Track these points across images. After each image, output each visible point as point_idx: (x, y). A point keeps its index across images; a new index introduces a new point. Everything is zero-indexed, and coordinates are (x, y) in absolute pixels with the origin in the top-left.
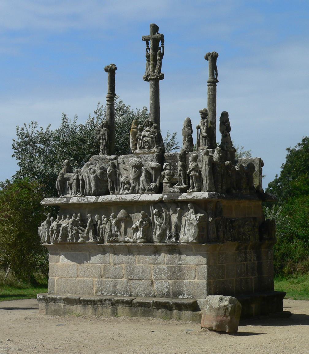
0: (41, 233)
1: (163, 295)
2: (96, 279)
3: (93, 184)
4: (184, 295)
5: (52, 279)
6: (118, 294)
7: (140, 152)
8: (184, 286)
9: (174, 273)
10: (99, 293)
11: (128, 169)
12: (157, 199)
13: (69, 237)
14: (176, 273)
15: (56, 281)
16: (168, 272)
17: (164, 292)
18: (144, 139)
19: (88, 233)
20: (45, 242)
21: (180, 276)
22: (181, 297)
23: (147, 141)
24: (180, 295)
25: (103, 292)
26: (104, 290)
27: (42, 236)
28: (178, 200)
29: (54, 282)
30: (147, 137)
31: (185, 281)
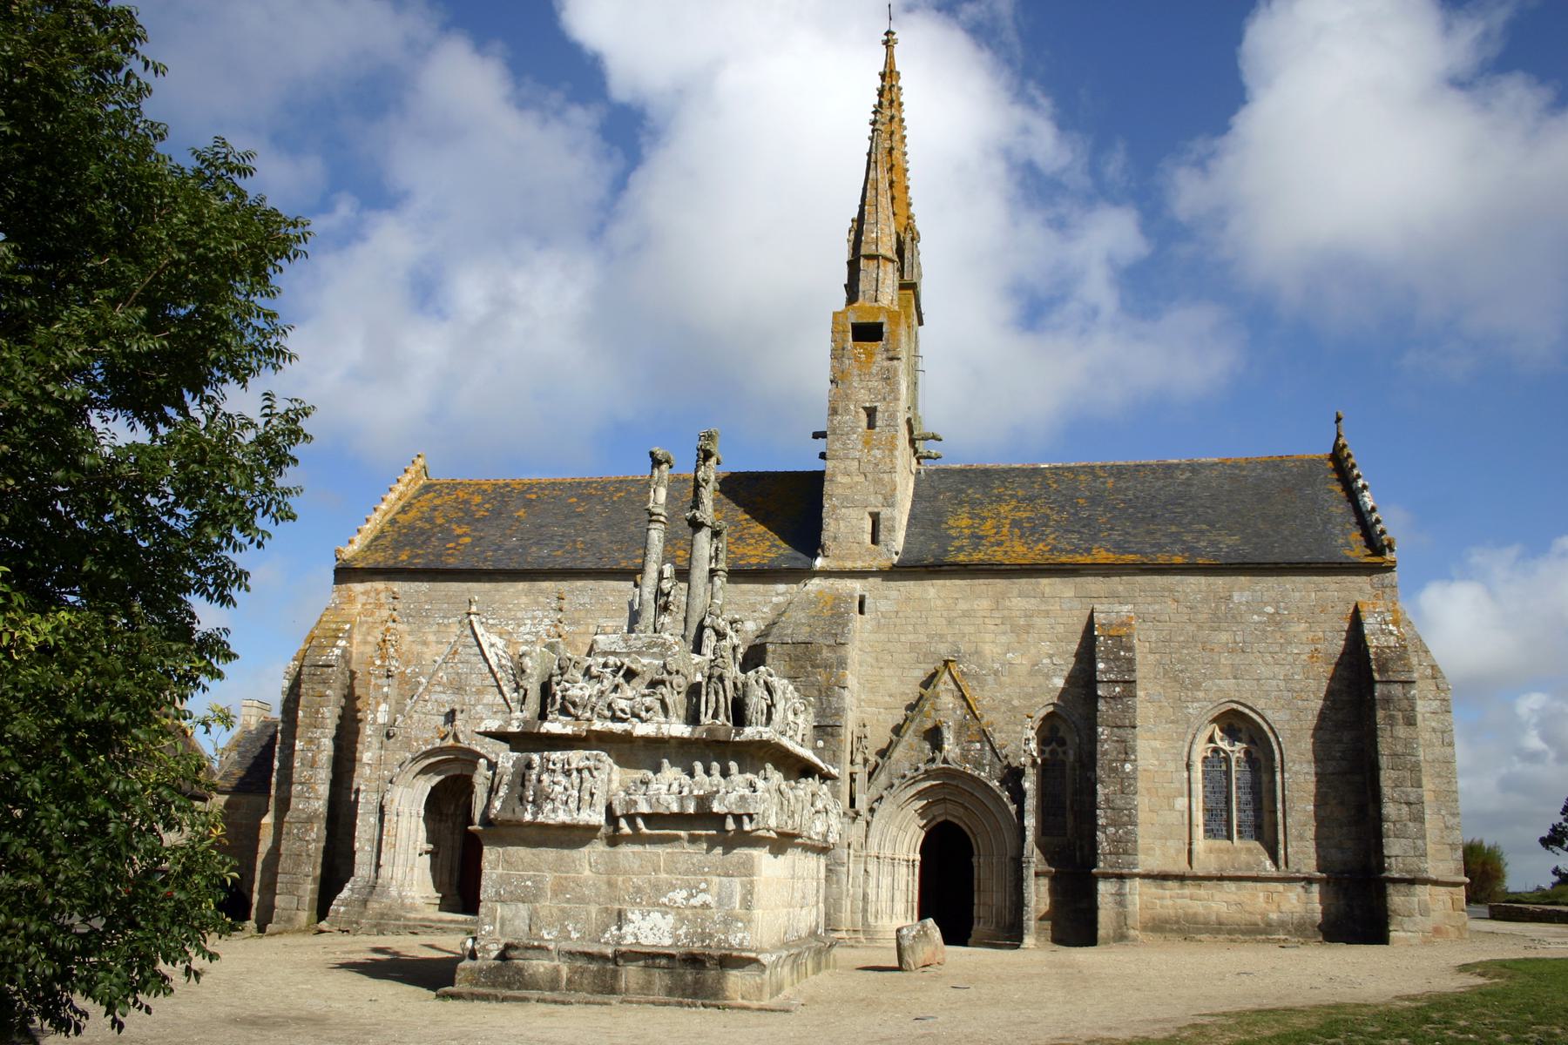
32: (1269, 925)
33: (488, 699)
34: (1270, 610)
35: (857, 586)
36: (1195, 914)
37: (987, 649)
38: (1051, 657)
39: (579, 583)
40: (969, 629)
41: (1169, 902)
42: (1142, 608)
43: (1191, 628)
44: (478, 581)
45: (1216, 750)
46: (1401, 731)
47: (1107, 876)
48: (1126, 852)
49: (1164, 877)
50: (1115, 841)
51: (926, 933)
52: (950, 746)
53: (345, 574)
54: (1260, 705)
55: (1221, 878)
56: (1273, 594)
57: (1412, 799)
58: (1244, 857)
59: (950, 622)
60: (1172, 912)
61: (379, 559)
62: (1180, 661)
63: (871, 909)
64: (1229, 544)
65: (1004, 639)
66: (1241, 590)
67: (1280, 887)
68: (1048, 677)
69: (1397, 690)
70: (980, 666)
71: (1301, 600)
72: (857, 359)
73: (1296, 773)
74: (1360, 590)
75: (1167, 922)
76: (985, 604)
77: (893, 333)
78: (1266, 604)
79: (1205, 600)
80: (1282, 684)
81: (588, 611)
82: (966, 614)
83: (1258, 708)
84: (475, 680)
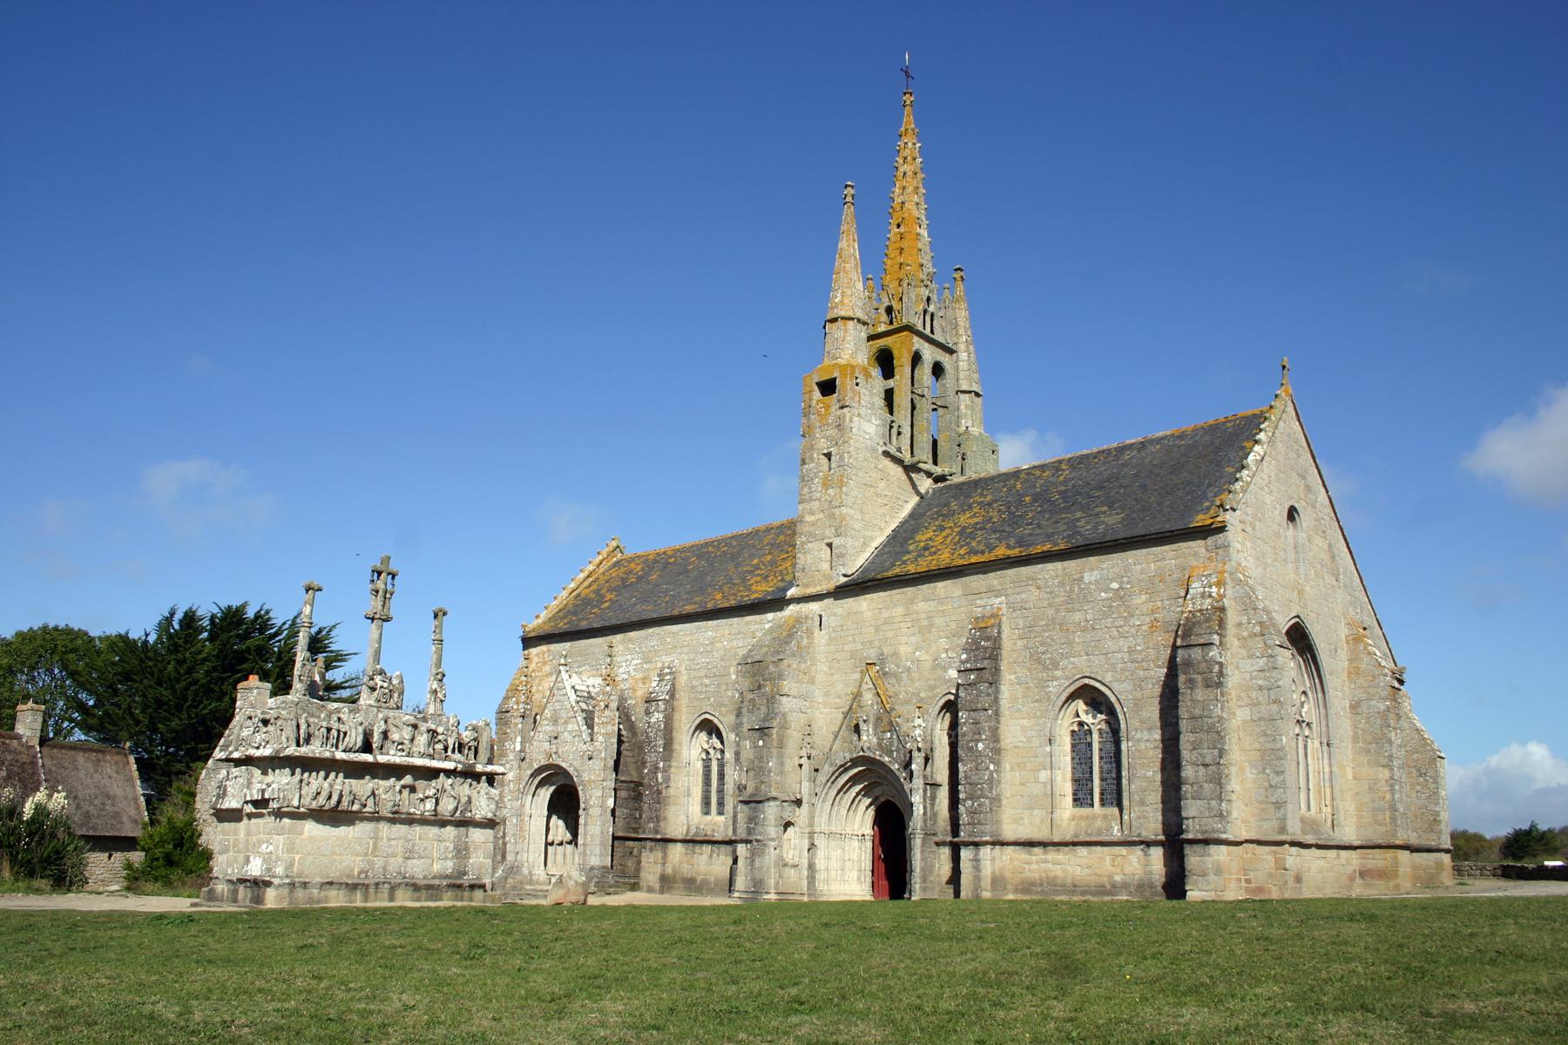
1: (446, 877)
9: (459, 851)
14: (462, 851)
32: (1114, 886)
33: (570, 727)
34: (1115, 585)
35: (814, 607)
36: (1055, 878)
37: (903, 650)
38: (946, 651)
40: (890, 634)
41: (1035, 867)
42: (1012, 599)
43: (1050, 612)
45: (1081, 724)
46: (1200, 694)
47: (967, 844)
48: (979, 823)
49: (1030, 844)
50: (973, 812)
52: (869, 737)
53: (529, 642)
54: (1108, 678)
55: (1075, 844)
56: (1117, 570)
57: (1208, 760)
58: (1099, 823)
59: (877, 630)
60: (1037, 876)
61: (562, 626)
62: (1042, 644)
63: (820, 876)
64: (1111, 522)
65: (913, 639)
66: (1091, 570)
67: (1123, 850)
68: (945, 669)
69: (1196, 653)
70: (898, 666)
71: (1142, 572)
72: (819, 413)
73: (1139, 741)
74: (1196, 555)
75: (1033, 884)
76: (900, 610)
77: (843, 383)
78: (1112, 580)
79: (1062, 584)
80: (1126, 656)
82: (887, 622)
83: (1106, 681)
84: (563, 714)
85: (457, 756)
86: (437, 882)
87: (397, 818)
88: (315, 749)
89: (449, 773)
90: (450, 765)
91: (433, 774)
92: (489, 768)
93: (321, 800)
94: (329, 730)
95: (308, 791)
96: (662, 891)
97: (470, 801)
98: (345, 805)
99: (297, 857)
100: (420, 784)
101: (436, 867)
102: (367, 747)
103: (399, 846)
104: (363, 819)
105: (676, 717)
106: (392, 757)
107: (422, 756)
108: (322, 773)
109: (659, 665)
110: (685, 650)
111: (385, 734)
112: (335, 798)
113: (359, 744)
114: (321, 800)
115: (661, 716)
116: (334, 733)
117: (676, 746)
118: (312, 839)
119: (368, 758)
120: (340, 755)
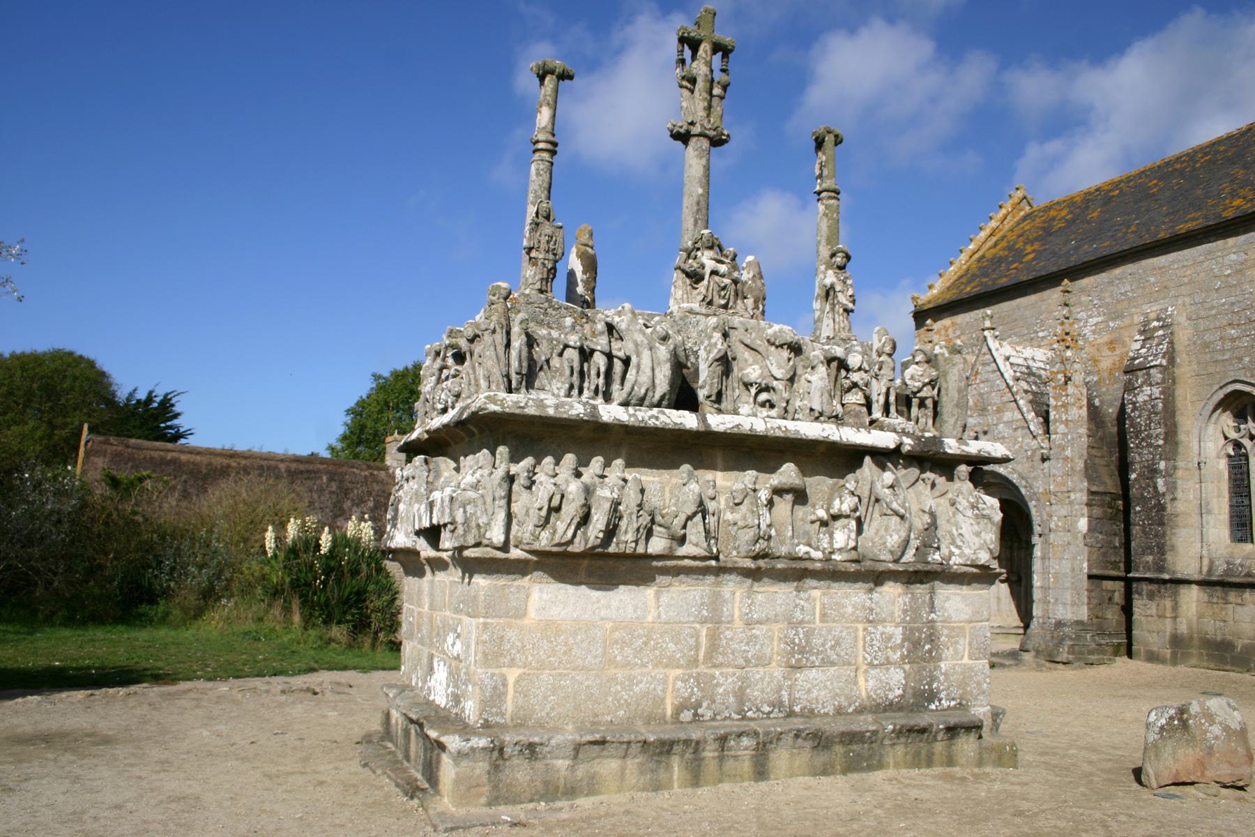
0: (465, 512)
2: (679, 672)
3: (663, 377)
4: (940, 700)
5: (493, 675)
6: (749, 714)
7: (704, 311)
8: (942, 678)
9: (916, 644)
10: (687, 716)
11: (760, 349)
12: (892, 446)
13: (626, 532)
14: (922, 644)
15: (511, 681)
16: (904, 640)
17: (891, 697)
18: (717, 278)
19: (684, 527)
20: (478, 545)
21: (930, 651)
22: (933, 707)
23: (724, 288)
24: (931, 701)
25: (700, 711)
26: (705, 705)
27: (473, 524)
28: (945, 453)
29: (505, 685)
30: (723, 276)
31: (942, 665)
33: (1008, 416)
39: (1117, 271)
44: (1025, 295)
51: (1184, 725)
81: (1129, 299)
84: (995, 398)
85: (897, 420)
86: (866, 723)
87: (766, 567)
88: (551, 399)
89: (883, 457)
90: (886, 440)
91: (845, 459)
92: (973, 448)
93: (562, 527)
94: (586, 355)
95: (529, 504)
96: (1174, 661)
97: (933, 525)
98: (626, 540)
99: (512, 675)
100: (818, 485)
101: (867, 686)
102: (683, 396)
103: (772, 640)
104: (677, 572)
105: (1179, 392)
106: (748, 419)
107: (819, 417)
108: (570, 459)
109: (1138, 319)
110: (1184, 290)
111: (725, 363)
112: (599, 521)
113: (662, 386)
114: (562, 527)
115: (1156, 391)
116: (600, 361)
117: (1182, 437)
118: (549, 628)
119: (687, 420)
120: (611, 413)
